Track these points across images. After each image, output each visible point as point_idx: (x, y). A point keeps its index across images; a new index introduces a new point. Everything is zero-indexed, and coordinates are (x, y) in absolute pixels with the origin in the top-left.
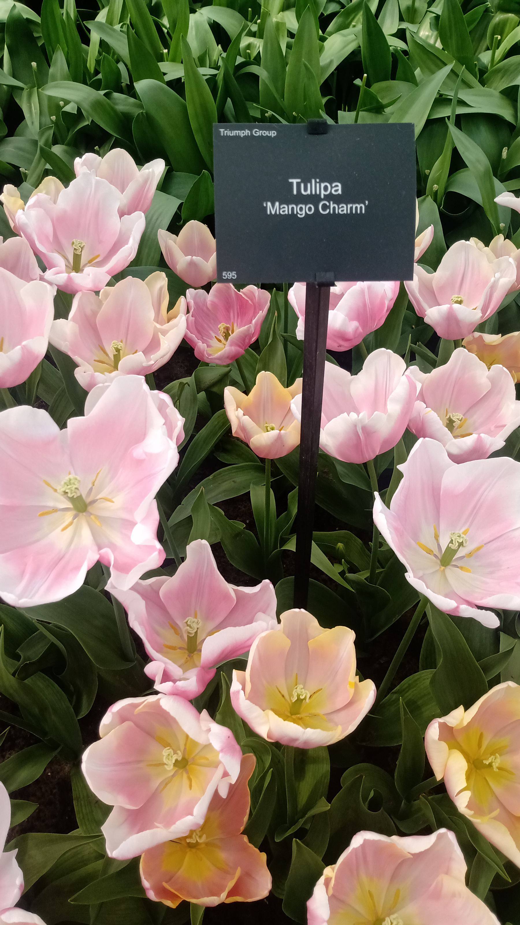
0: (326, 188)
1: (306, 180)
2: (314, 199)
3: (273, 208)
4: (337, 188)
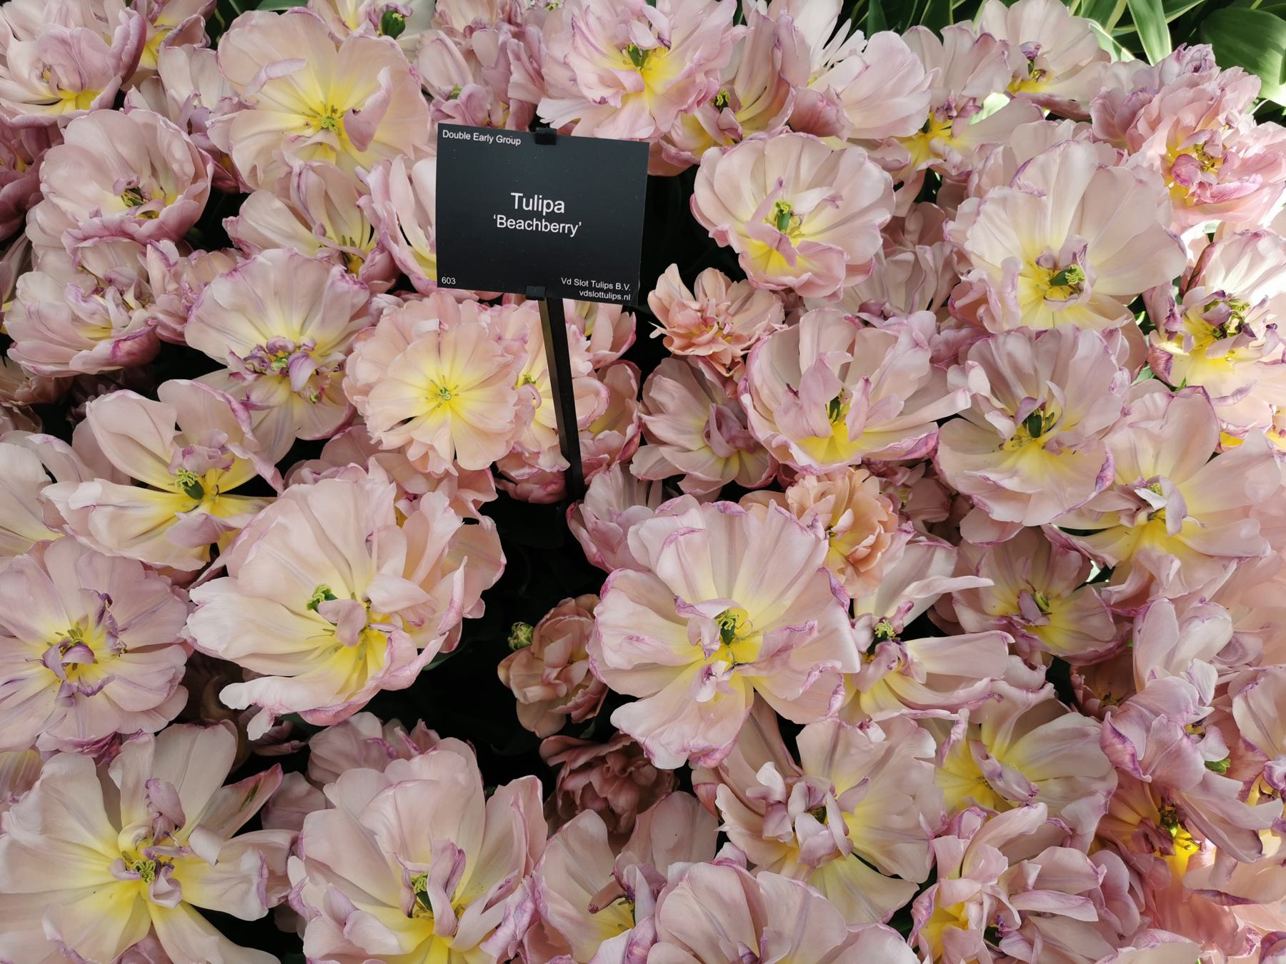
0: (548, 206)
1: (529, 196)
3: (502, 221)
4: (560, 207)
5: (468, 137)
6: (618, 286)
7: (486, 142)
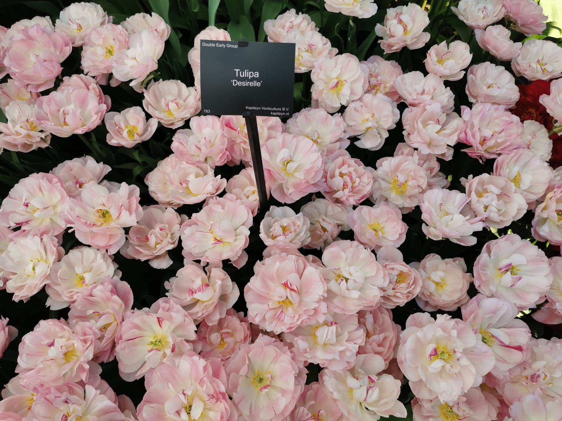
0: (251, 74)
1: (243, 70)
2: (245, 79)
5: (214, 45)
6: (284, 109)
7: (222, 47)
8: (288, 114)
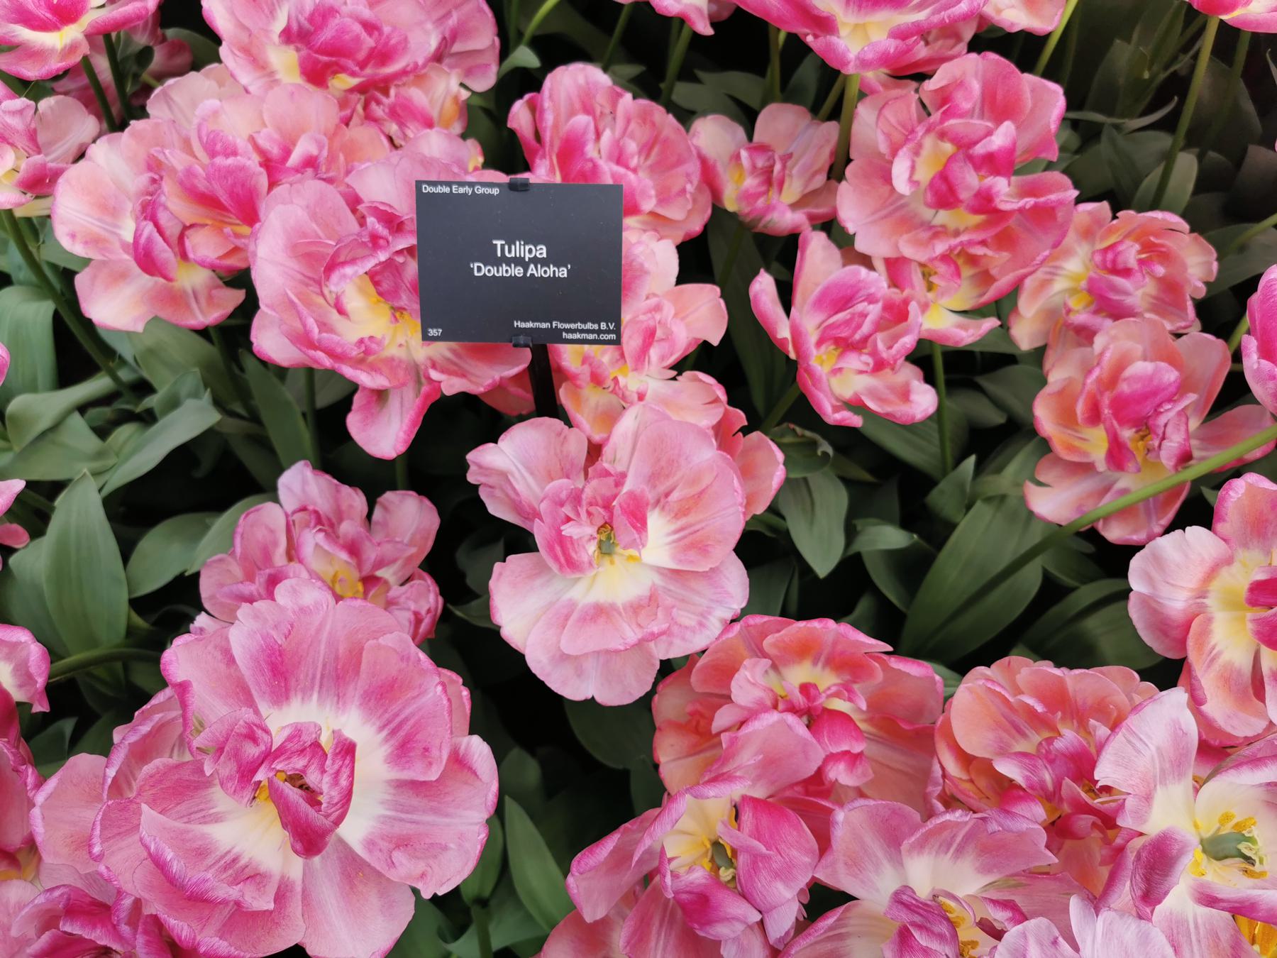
0: (530, 251)
1: (510, 242)
2: (519, 261)
3: (481, 270)
4: (542, 251)
8: (613, 336)
